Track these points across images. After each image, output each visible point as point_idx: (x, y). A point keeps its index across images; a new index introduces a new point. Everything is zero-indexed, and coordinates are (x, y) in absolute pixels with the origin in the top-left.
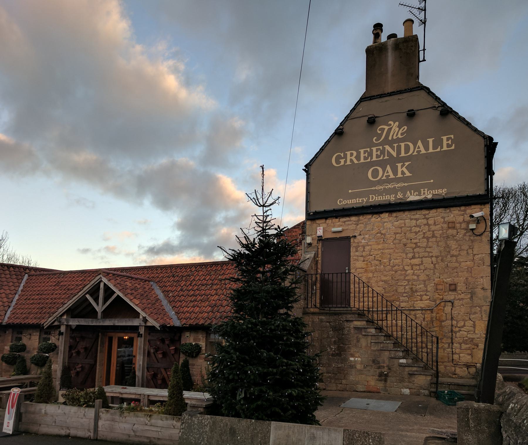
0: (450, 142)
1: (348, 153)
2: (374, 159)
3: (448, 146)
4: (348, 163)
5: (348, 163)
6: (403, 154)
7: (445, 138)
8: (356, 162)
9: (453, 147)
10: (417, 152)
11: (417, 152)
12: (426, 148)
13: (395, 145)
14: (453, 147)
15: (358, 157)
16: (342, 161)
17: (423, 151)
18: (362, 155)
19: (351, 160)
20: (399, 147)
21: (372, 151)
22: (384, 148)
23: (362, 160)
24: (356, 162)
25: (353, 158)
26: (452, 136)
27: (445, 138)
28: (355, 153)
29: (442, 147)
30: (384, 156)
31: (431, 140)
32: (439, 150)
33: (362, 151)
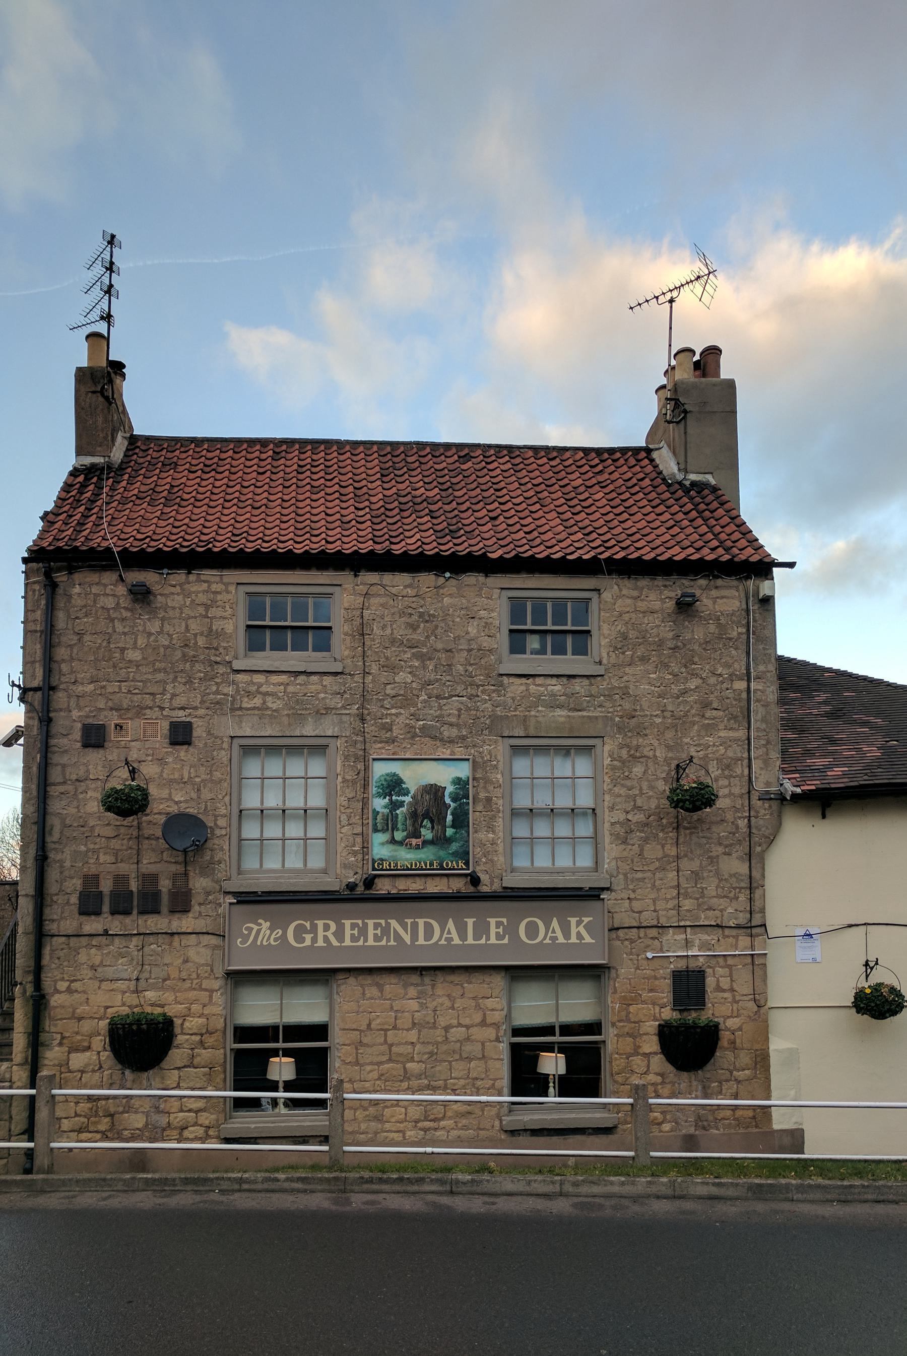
0: (501, 930)
1: (320, 923)
2: (371, 942)
3: (499, 937)
4: (320, 943)
5: (320, 943)
6: (421, 941)
7: (493, 921)
8: (335, 943)
9: (506, 941)
10: (446, 939)
11: (446, 939)
12: (463, 935)
13: (409, 921)
14: (506, 941)
15: (339, 935)
16: (308, 938)
17: (457, 941)
18: (348, 932)
19: (326, 939)
20: (415, 926)
21: (365, 925)
22: (388, 924)
23: (347, 942)
24: (335, 943)
25: (329, 934)
26: (505, 920)
27: (493, 921)
28: (333, 926)
29: (488, 939)
30: (388, 940)
31: (470, 922)
32: (483, 941)
33: (347, 923)
